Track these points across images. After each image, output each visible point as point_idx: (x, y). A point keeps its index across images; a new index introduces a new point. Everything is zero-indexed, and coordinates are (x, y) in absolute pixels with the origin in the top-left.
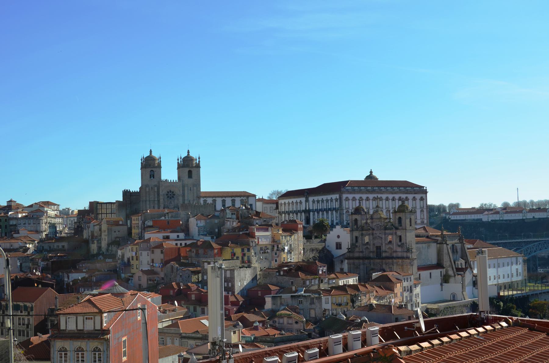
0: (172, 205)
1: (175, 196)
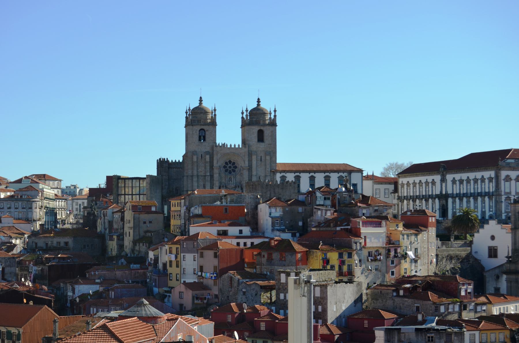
0: (233, 182)
1: (236, 170)
